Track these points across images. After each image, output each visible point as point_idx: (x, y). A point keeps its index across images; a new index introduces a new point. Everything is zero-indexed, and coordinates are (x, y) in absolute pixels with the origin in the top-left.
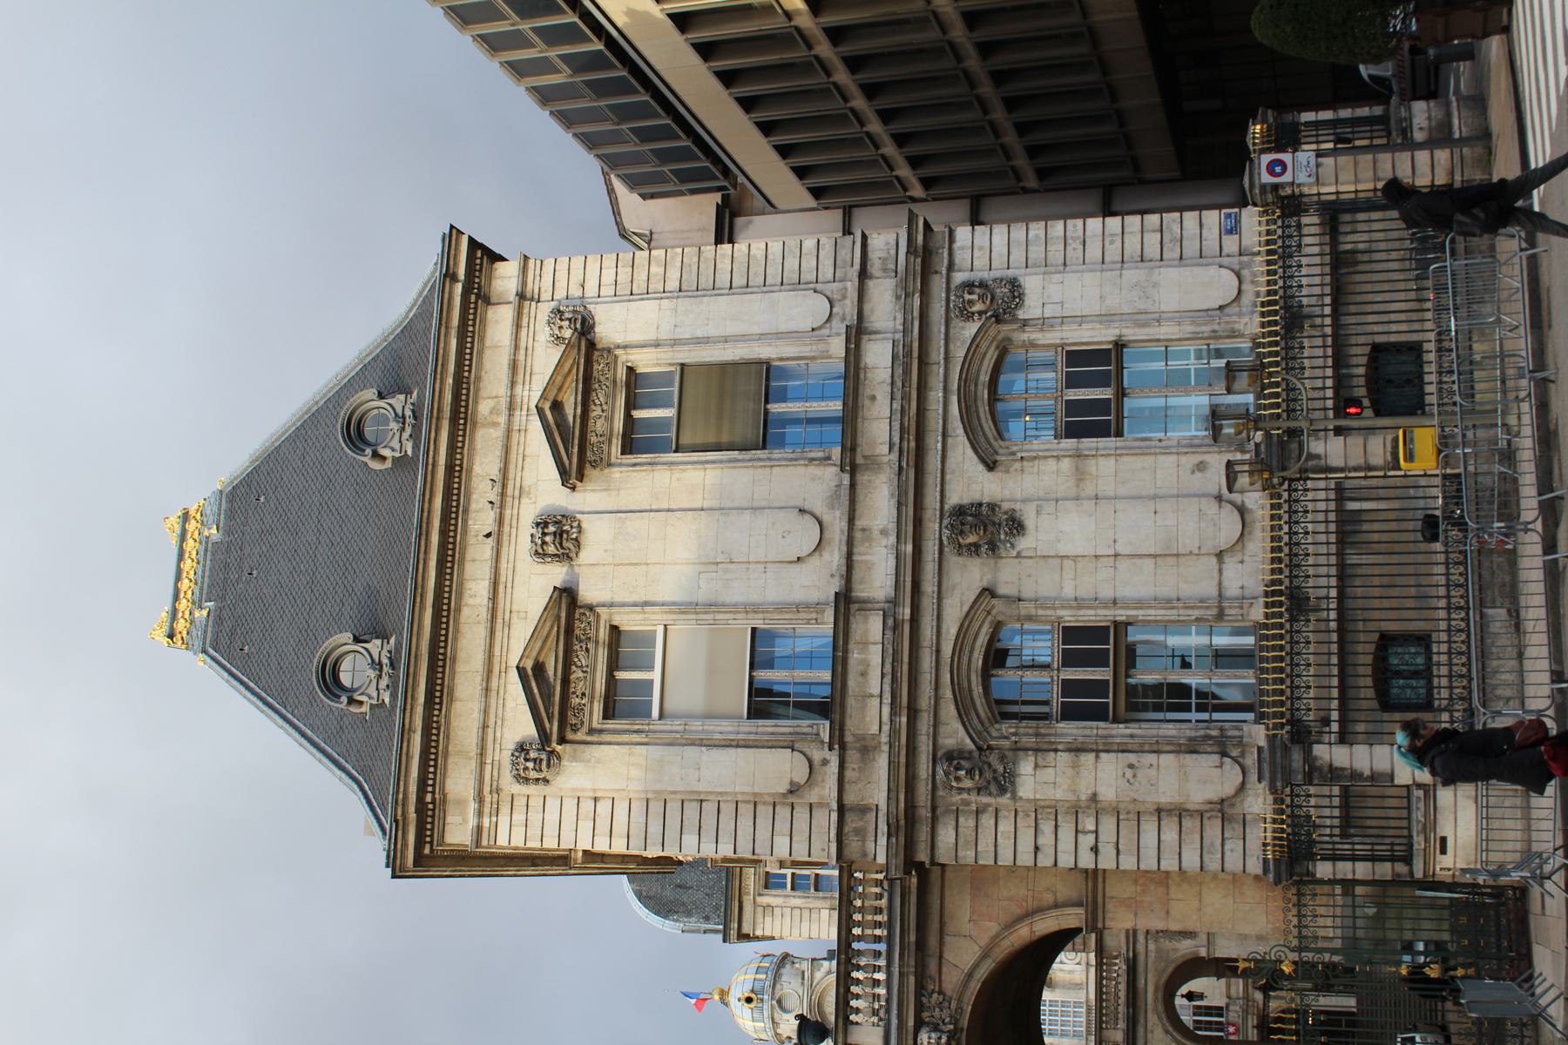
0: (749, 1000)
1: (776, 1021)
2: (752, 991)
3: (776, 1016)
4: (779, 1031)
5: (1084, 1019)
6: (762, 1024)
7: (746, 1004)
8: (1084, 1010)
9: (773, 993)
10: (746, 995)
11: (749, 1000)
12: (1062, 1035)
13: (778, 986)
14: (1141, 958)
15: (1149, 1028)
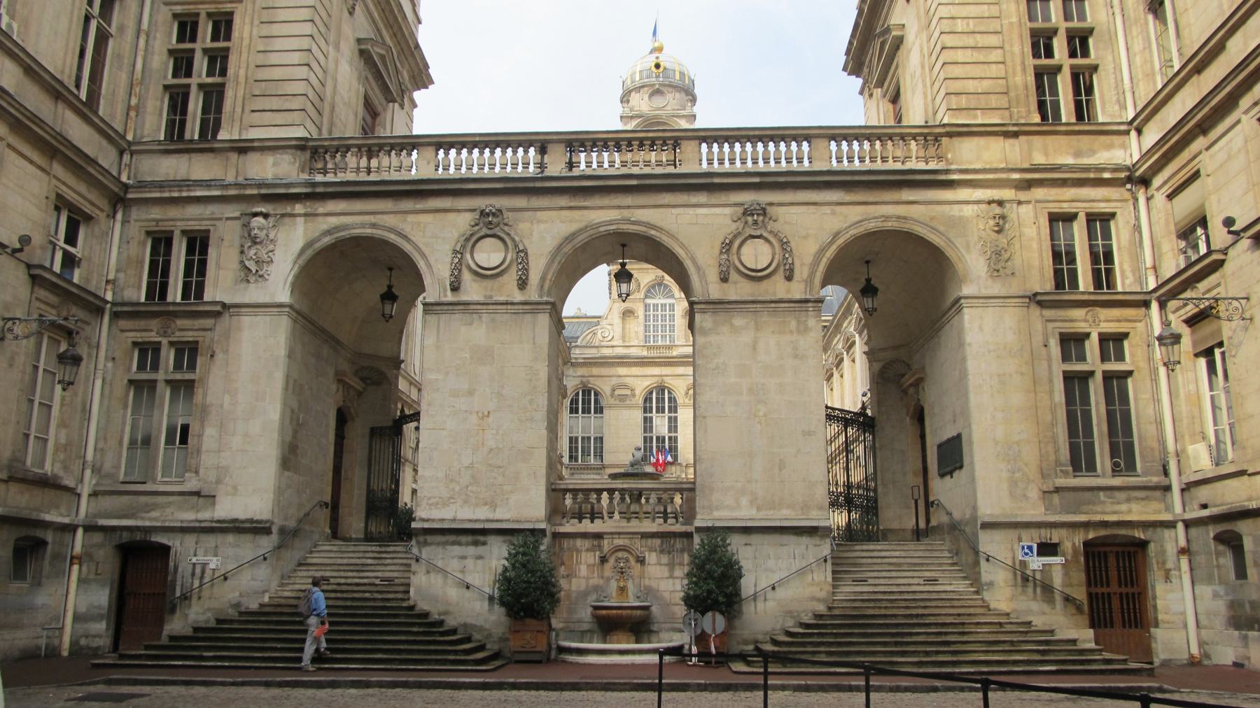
0: (657, 66)
1: (642, 91)
2: (665, 68)
3: (646, 89)
4: (633, 94)
5: (660, 343)
6: (638, 79)
7: (653, 64)
8: (668, 343)
9: (665, 85)
10: (662, 64)
11: (657, 66)
12: (646, 326)
13: (670, 90)
14: (948, 195)
15: (839, 209)
